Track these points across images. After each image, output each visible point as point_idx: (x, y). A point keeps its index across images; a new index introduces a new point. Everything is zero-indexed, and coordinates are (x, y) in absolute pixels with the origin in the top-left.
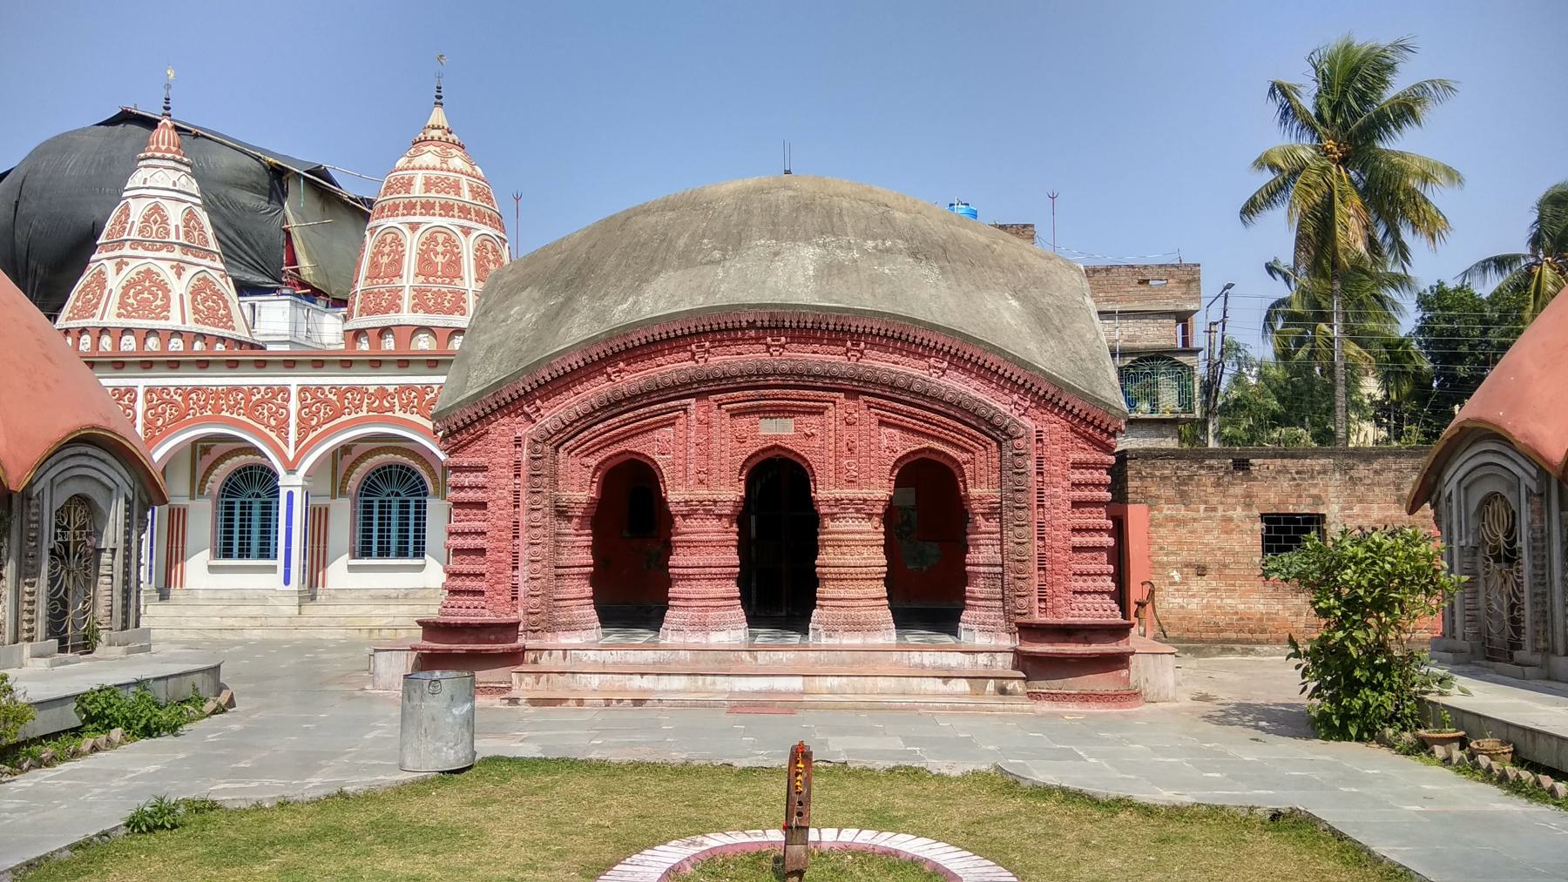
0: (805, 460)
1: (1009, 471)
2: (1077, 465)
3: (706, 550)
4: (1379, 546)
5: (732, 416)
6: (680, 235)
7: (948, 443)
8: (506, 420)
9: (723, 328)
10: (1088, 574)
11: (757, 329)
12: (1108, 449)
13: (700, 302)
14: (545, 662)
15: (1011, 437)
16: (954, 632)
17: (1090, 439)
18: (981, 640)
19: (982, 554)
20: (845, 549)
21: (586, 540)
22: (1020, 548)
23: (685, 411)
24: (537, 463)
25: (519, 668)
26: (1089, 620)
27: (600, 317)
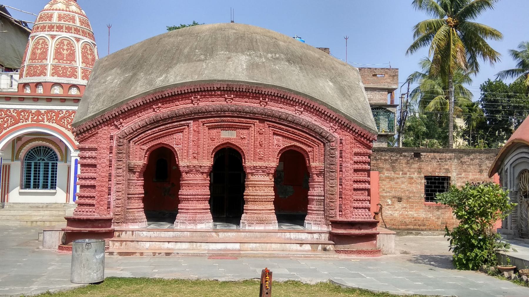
0: (241, 149)
1: (328, 156)
2: (356, 154)
3: (195, 187)
4: (483, 190)
5: (209, 129)
6: (185, 47)
7: (302, 143)
8: (106, 128)
9: (206, 90)
10: (360, 200)
11: (221, 91)
12: (369, 148)
13: (196, 78)
14: (124, 236)
15: (329, 141)
16: (302, 224)
17: (362, 143)
18: (315, 228)
19: (316, 191)
20: (257, 188)
21: (141, 182)
22: (332, 189)
23: (188, 126)
24: (120, 147)
25: (112, 239)
26: (360, 220)
27: (150, 83)
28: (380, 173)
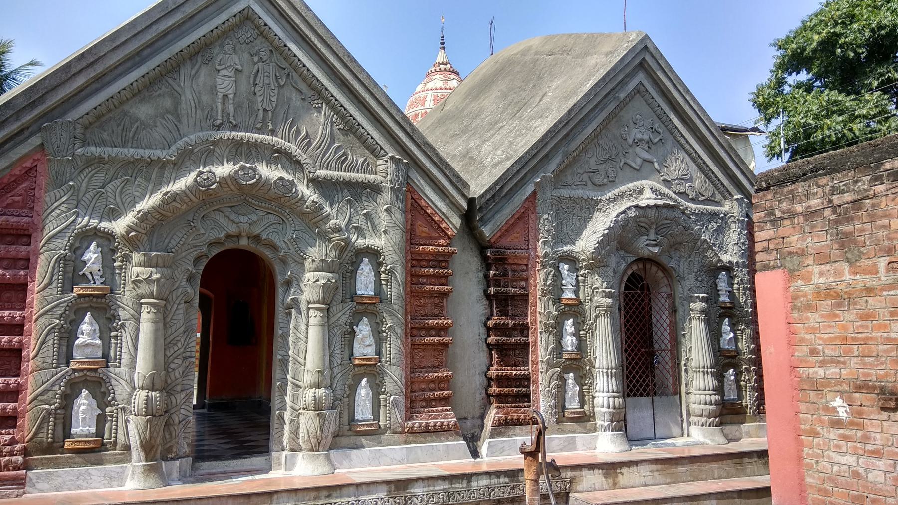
28: (792, 274)
